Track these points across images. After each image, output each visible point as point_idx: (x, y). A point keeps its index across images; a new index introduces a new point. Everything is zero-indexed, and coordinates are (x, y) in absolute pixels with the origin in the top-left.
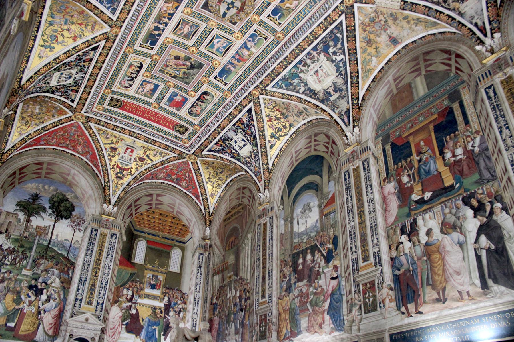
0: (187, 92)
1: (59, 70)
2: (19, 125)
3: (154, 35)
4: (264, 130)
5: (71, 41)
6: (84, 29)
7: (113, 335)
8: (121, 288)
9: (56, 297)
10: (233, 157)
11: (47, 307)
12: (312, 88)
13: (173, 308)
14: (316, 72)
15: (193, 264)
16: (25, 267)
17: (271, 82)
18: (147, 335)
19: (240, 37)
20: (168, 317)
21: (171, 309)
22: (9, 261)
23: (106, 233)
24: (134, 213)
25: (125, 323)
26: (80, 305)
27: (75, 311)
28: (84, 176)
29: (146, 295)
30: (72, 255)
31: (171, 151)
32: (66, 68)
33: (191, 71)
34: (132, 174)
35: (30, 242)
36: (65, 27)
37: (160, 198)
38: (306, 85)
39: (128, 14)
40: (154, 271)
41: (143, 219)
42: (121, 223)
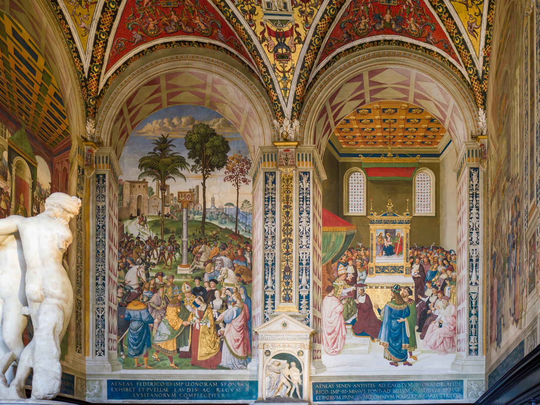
9: (235, 299)
11: (226, 317)
13: (430, 282)
16: (179, 263)
20: (423, 299)
21: (427, 284)
22: (155, 259)
23: (291, 174)
25: (349, 321)
26: (274, 304)
27: (267, 316)
28: (230, 80)
29: (379, 267)
30: (243, 228)
35: (175, 222)
40: (386, 222)
41: (351, 129)
42: (312, 148)
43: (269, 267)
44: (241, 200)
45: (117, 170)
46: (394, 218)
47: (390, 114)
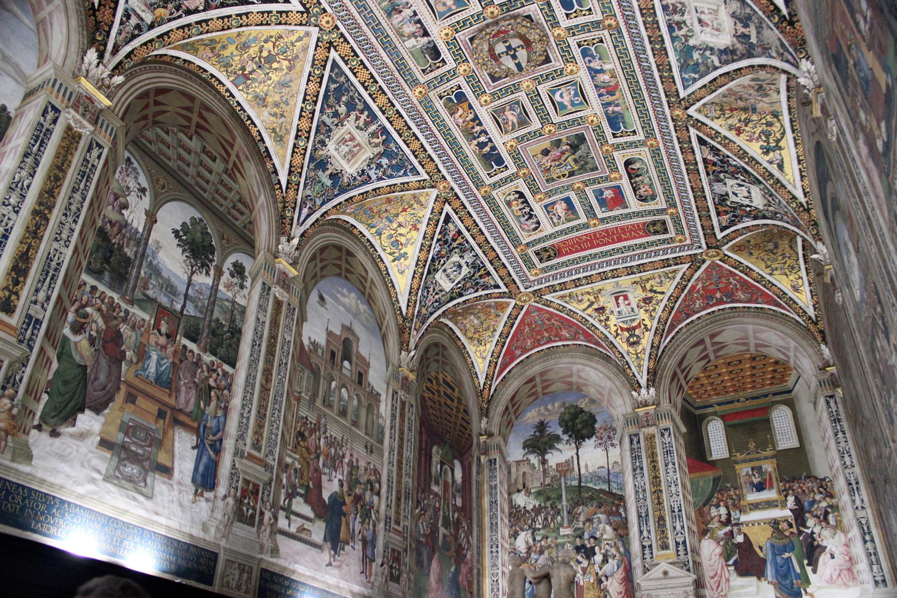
0: (607, 179)
1: (437, 270)
2: (474, 349)
3: (488, 153)
4: (745, 152)
5: (414, 233)
6: (413, 212)
7: (718, 587)
8: (706, 509)
10: (755, 218)
12: (722, 48)
13: (810, 512)
14: (700, 21)
15: (820, 421)
16: (561, 525)
17: (675, 85)
18: (777, 571)
19: (574, 68)
20: (806, 530)
24: (684, 383)
25: (731, 562)
26: (652, 553)
27: (647, 566)
29: (752, 504)
31: (677, 264)
32: (442, 262)
33: (579, 153)
34: (649, 327)
36: (395, 225)
37: (716, 339)
38: (712, 49)
39: (432, 160)
40: (751, 460)
41: (702, 385)
43: (642, 518)
44: (611, 462)
45: (505, 454)
46: (758, 455)
47: (736, 365)
